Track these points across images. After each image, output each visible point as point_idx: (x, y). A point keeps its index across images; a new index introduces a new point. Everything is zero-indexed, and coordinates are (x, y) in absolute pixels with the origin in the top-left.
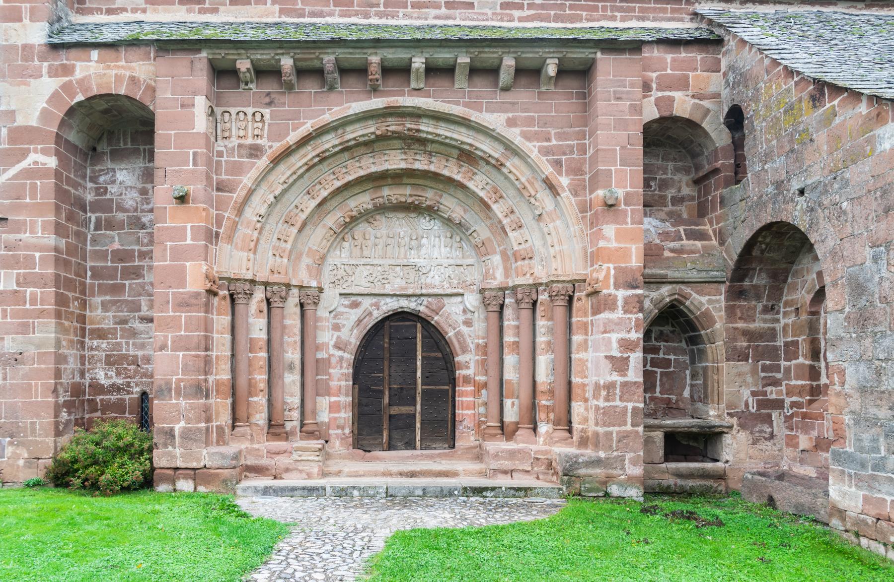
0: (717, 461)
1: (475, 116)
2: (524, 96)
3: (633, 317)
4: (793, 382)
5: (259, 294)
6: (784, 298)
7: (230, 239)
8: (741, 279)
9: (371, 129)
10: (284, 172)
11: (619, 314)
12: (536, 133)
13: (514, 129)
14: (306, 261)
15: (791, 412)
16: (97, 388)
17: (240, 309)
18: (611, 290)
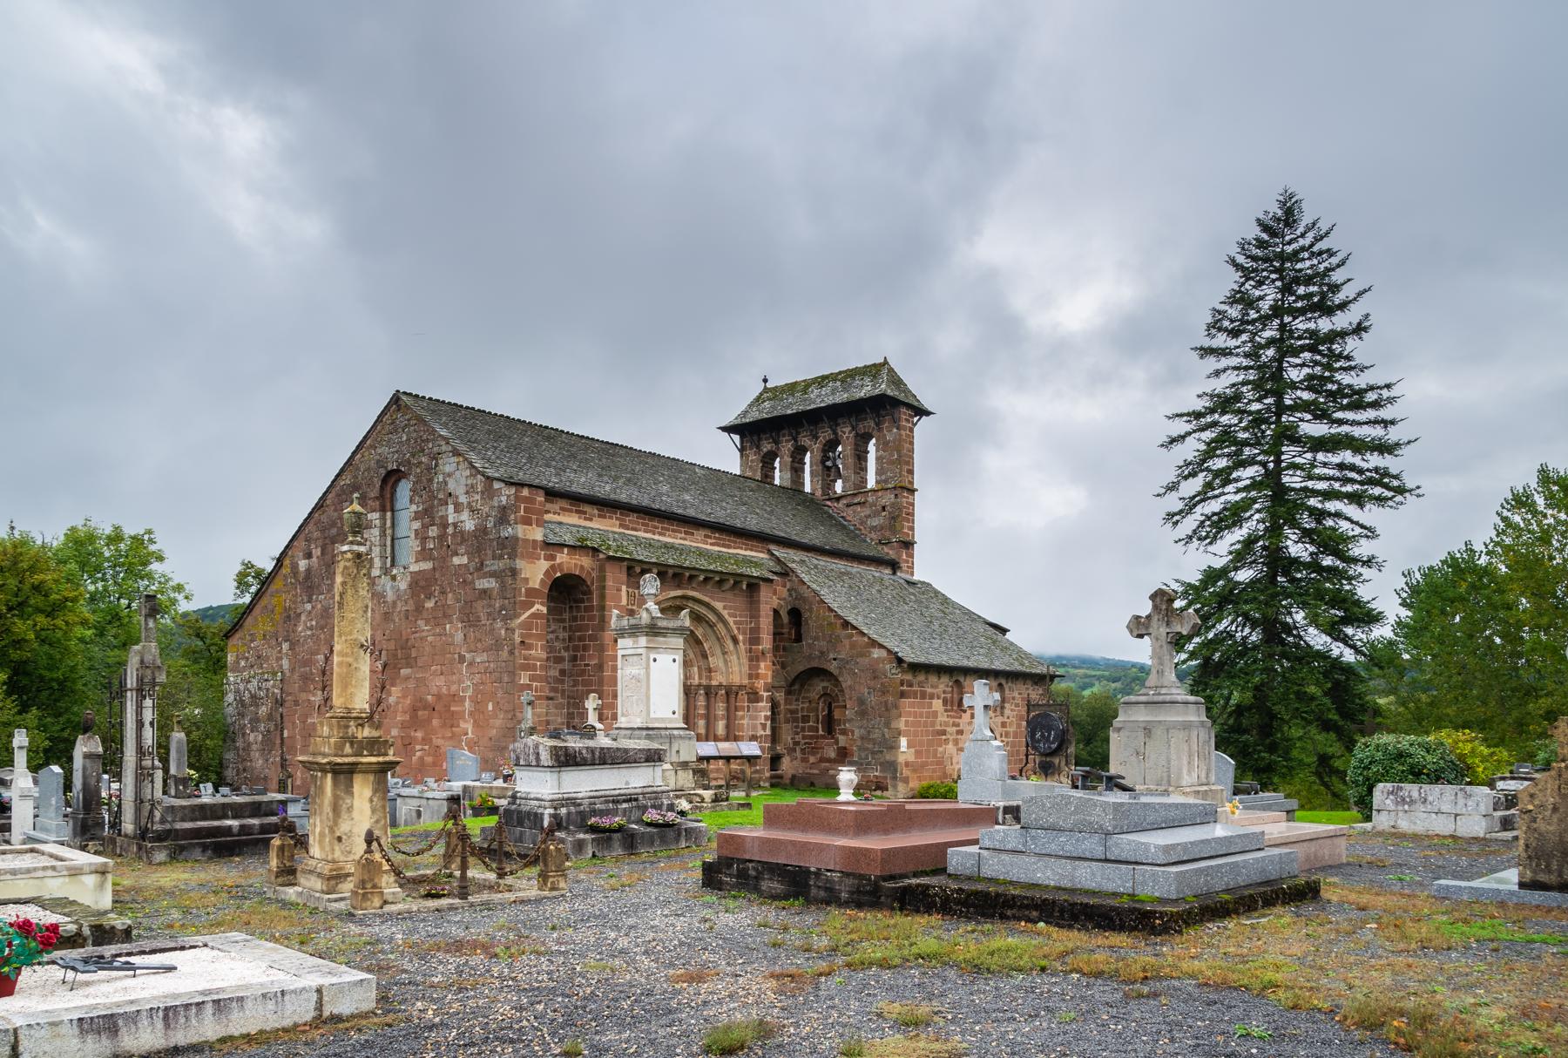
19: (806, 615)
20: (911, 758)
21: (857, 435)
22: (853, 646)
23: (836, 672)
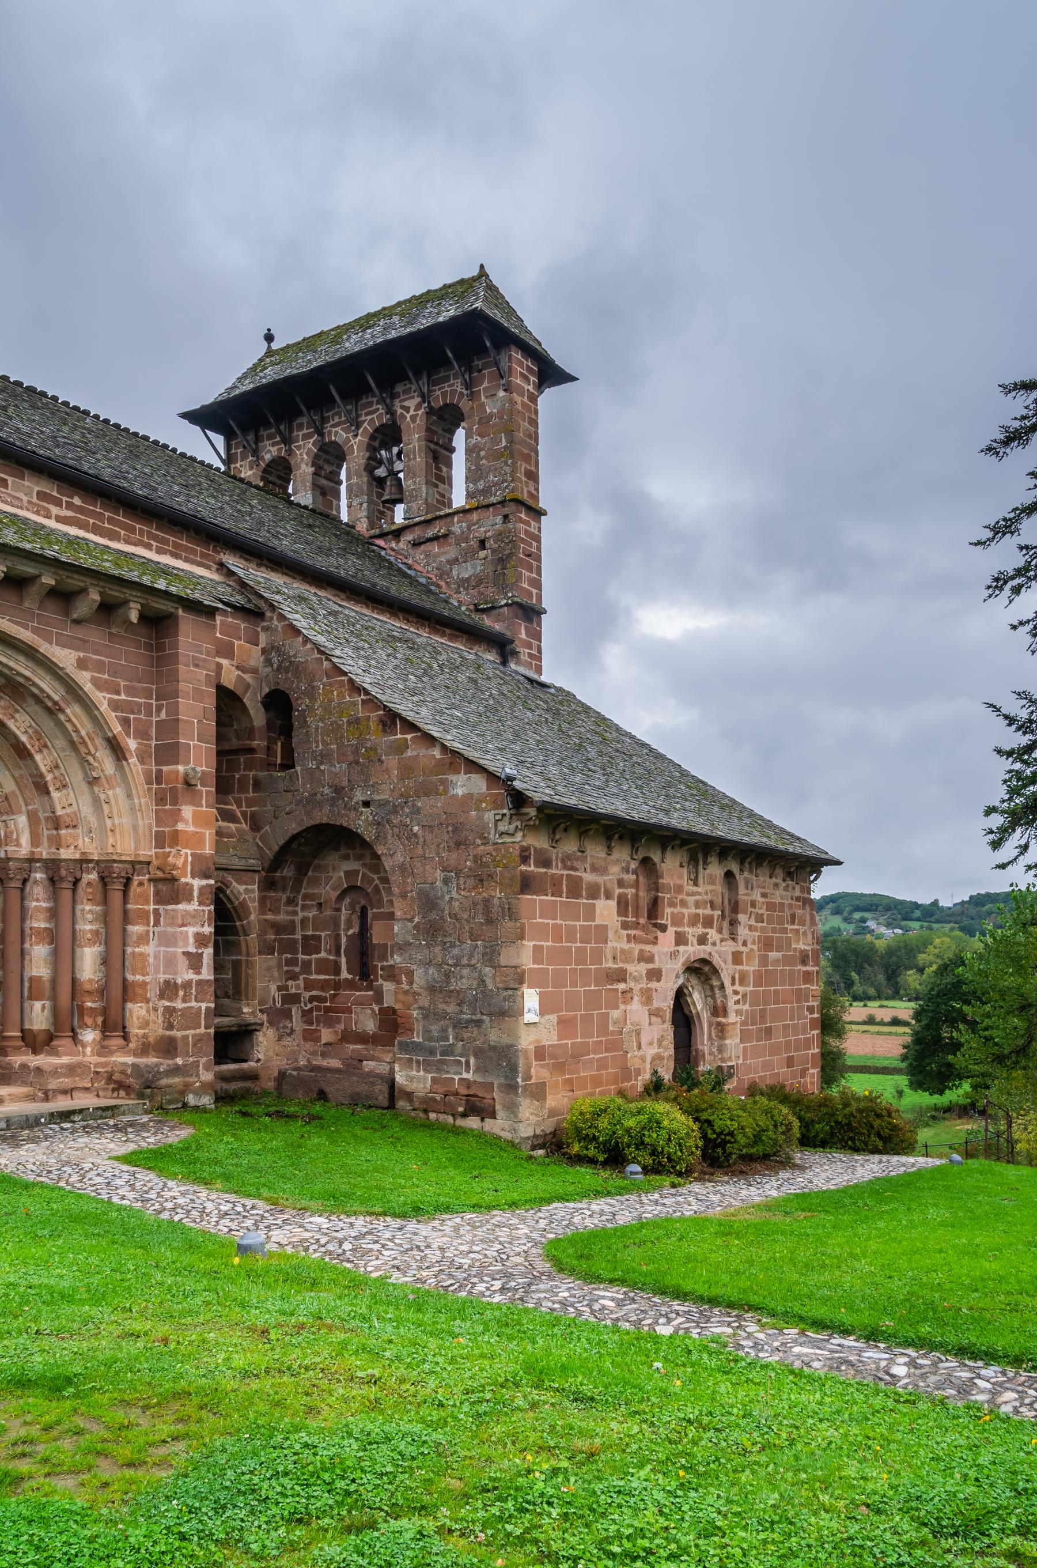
0: (246, 1061)
2: (95, 635)
3: (206, 909)
4: (314, 977)
6: (303, 891)
8: (275, 871)
12: (106, 681)
13: (84, 673)
15: (309, 1006)
18: (188, 879)
19: (301, 704)
20: (549, 1037)
21: (431, 411)
22: (407, 770)
23: (369, 834)
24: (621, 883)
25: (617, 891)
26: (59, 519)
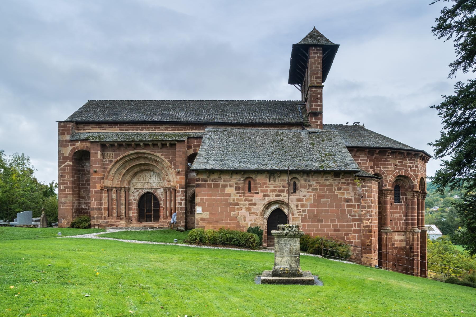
1: (155, 154)
5: (114, 190)
7: (107, 179)
9: (135, 156)
10: (118, 165)
11: (180, 194)
14: (126, 182)
16: (82, 209)
17: (110, 193)
20: (206, 215)
24: (236, 183)
25: (235, 185)
26: (170, 130)
